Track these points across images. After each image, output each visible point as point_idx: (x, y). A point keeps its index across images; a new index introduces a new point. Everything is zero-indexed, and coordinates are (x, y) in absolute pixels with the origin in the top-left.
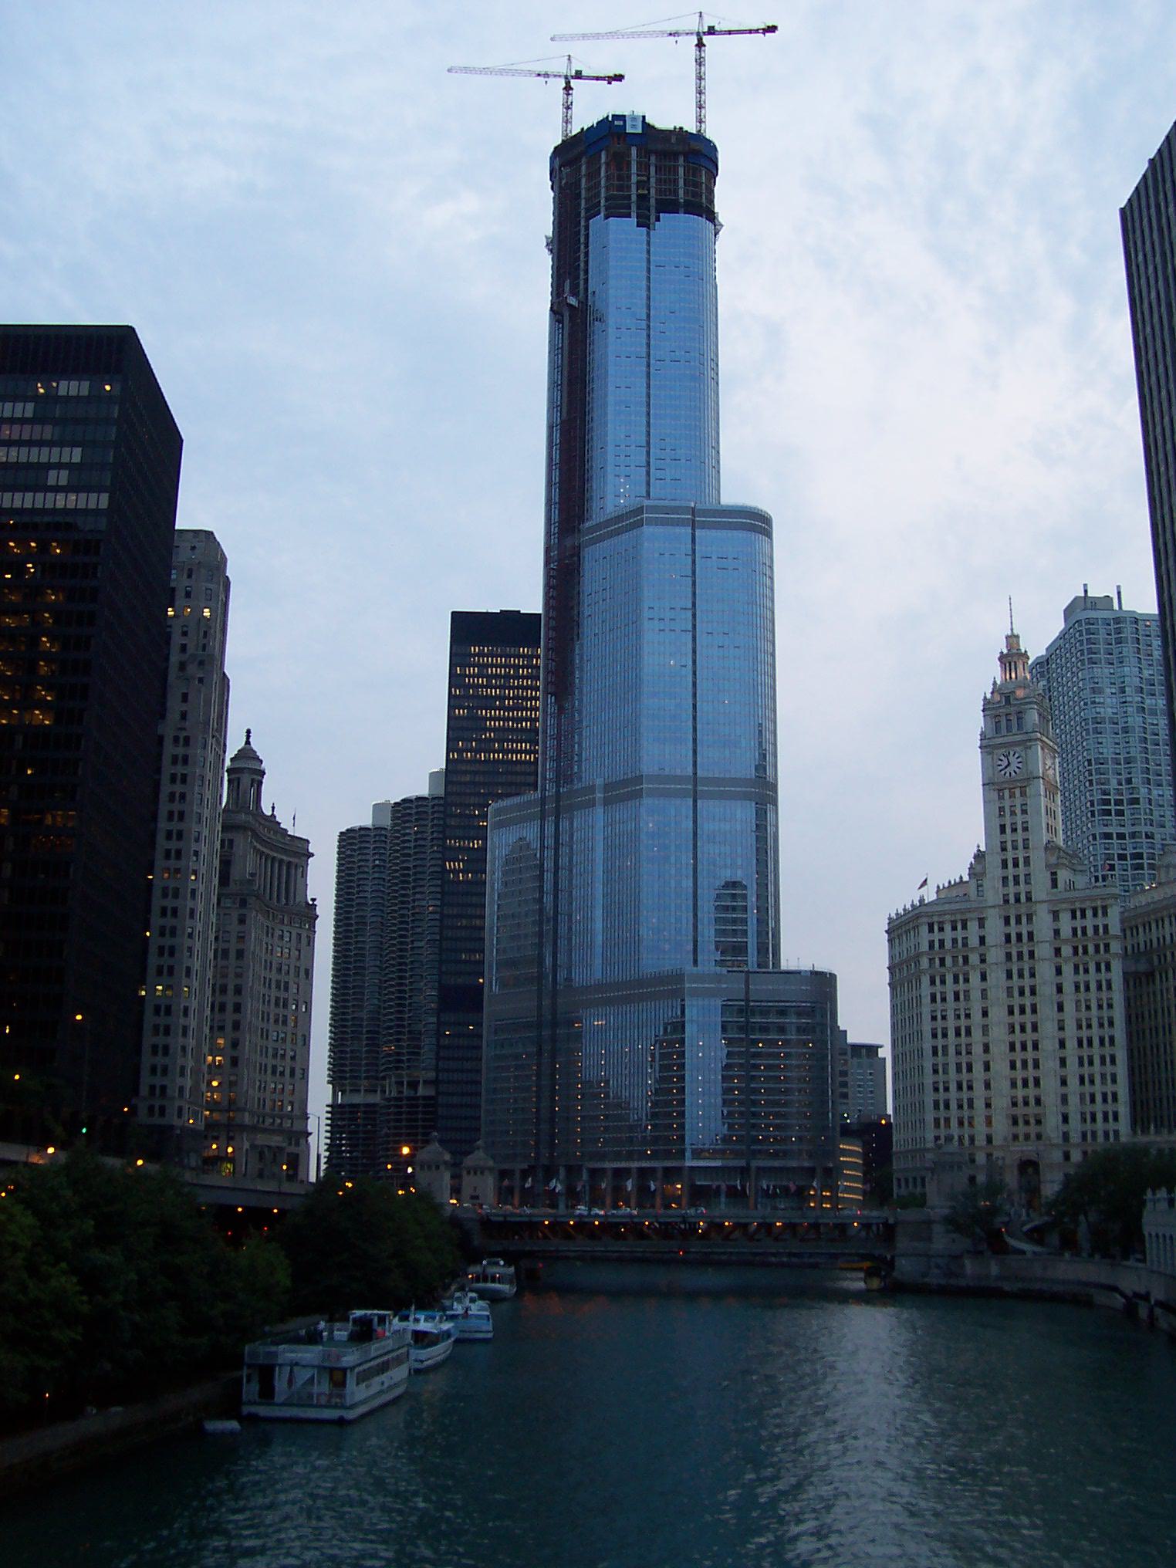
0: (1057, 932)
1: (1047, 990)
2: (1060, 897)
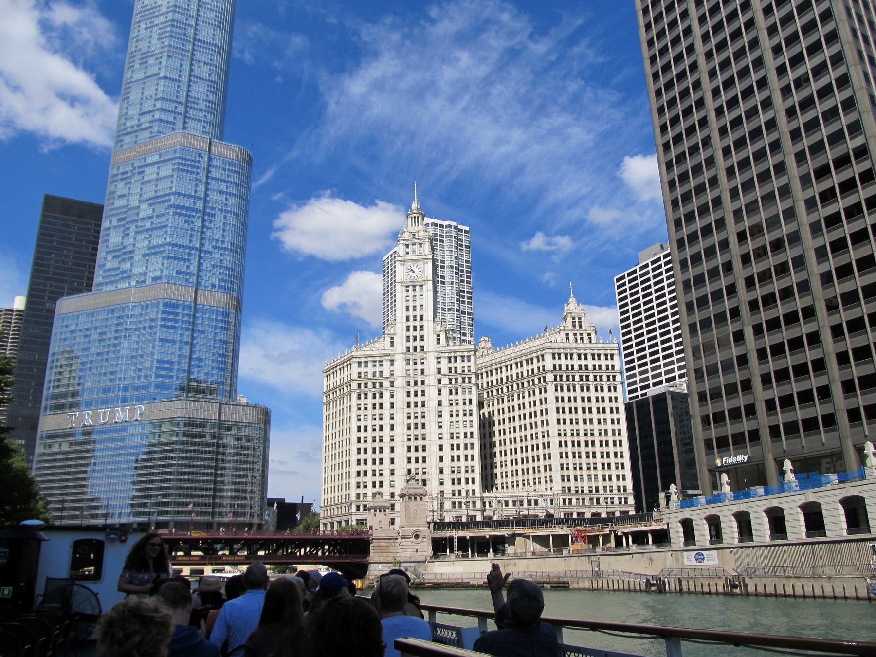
2: (442, 349)
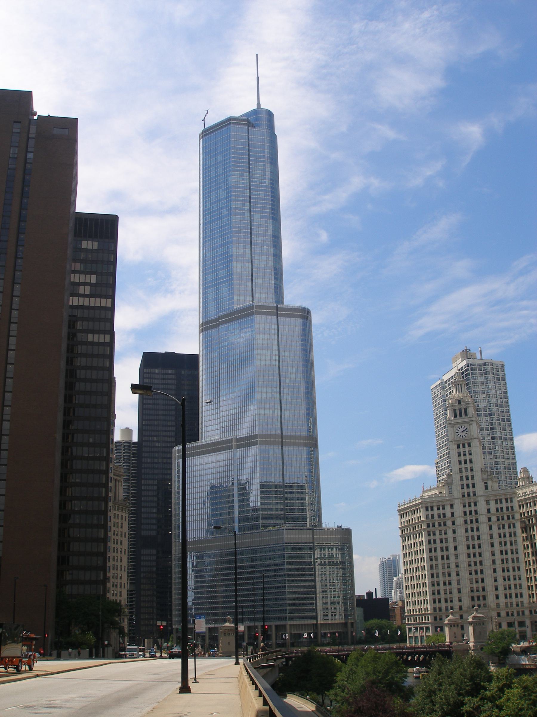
0: (489, 511)
1: (485, 537)
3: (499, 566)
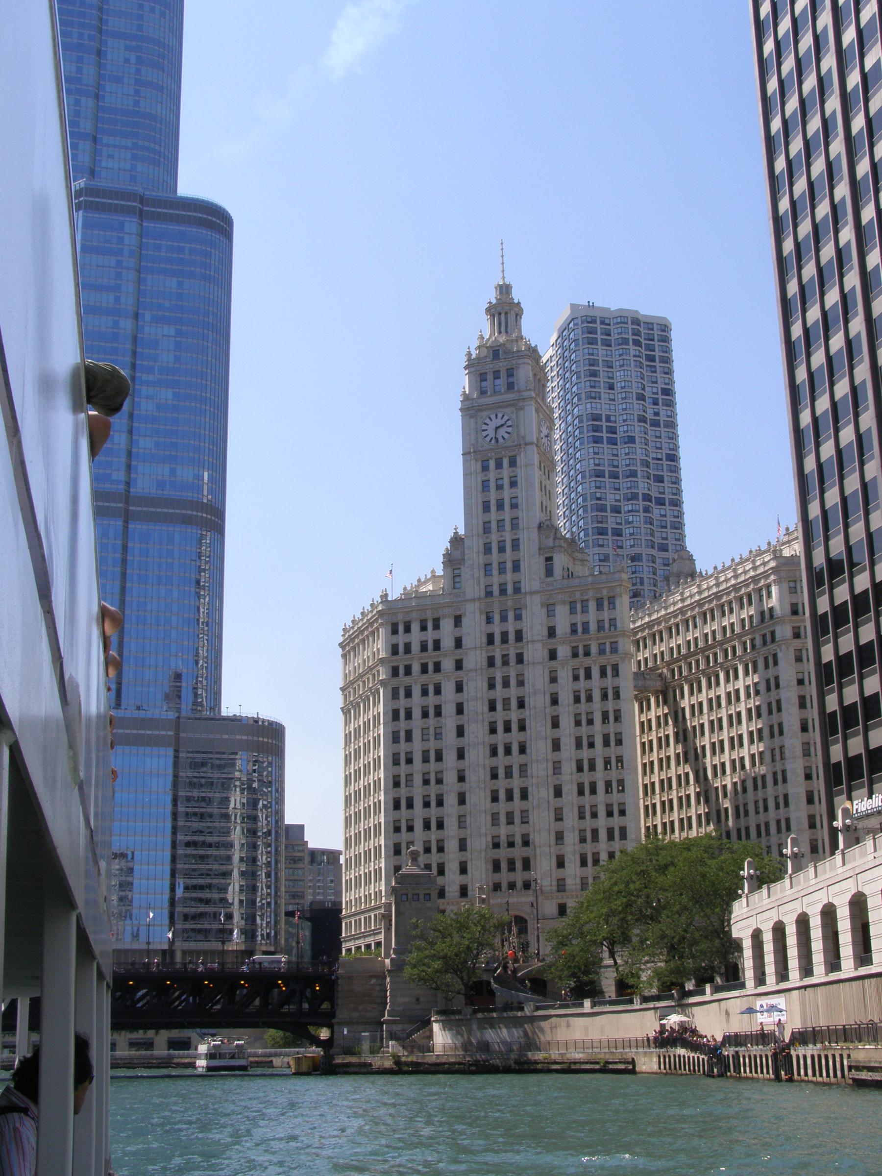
0: (552, 632)
1: (538, 702)
3: (569, 778)
